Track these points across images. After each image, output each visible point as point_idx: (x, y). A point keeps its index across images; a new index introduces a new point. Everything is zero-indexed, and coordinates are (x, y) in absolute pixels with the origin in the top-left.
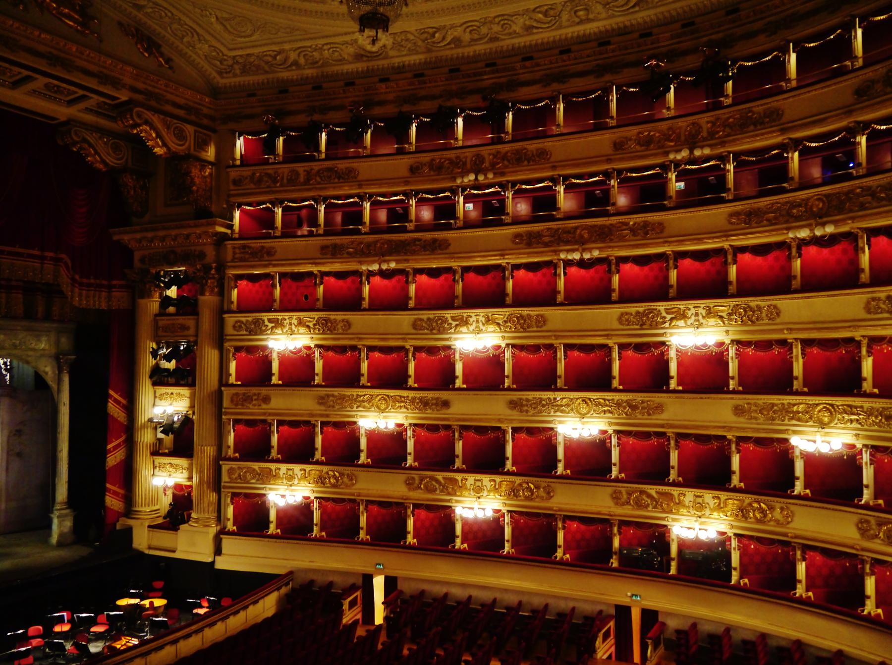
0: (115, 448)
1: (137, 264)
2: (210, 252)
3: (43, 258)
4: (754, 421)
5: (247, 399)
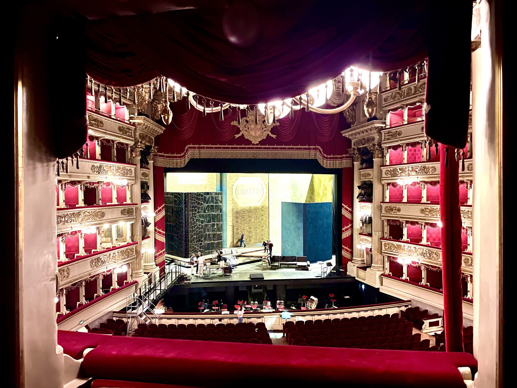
0: (346, 230)
1: (353, 146)
2: (377, 137)
3: (310, 149)
5: (392, 210)
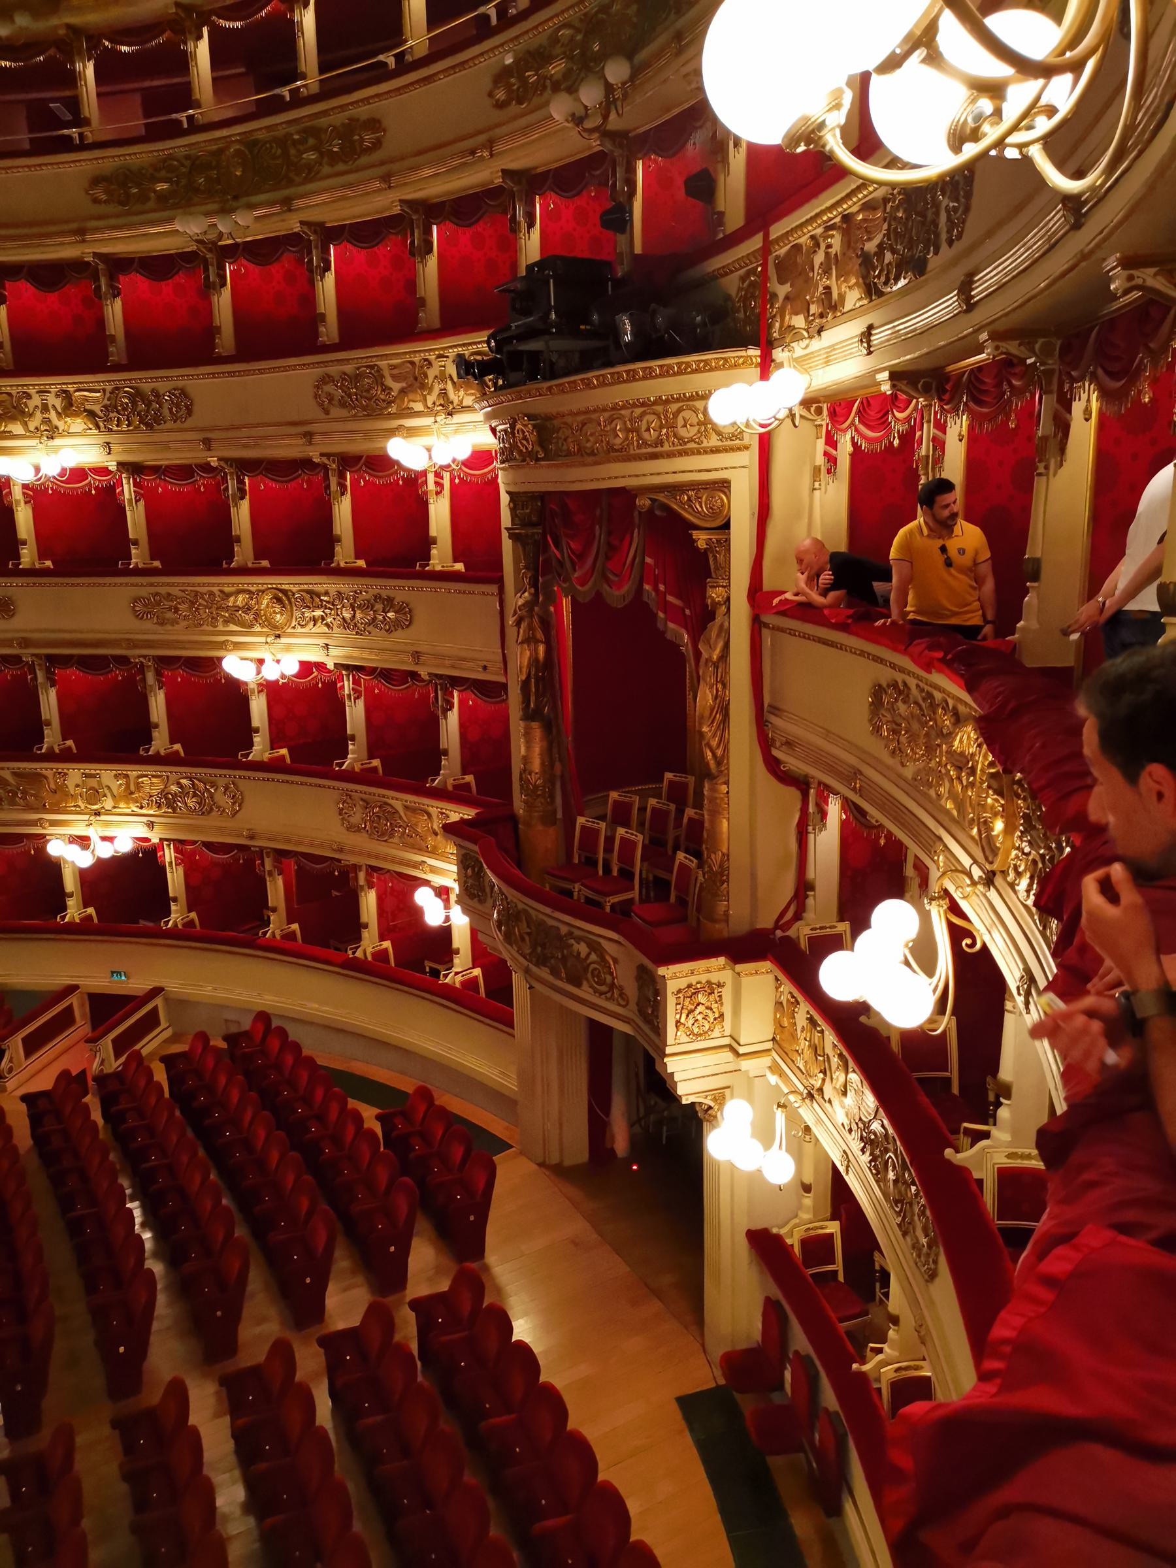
4: (169, 627)
